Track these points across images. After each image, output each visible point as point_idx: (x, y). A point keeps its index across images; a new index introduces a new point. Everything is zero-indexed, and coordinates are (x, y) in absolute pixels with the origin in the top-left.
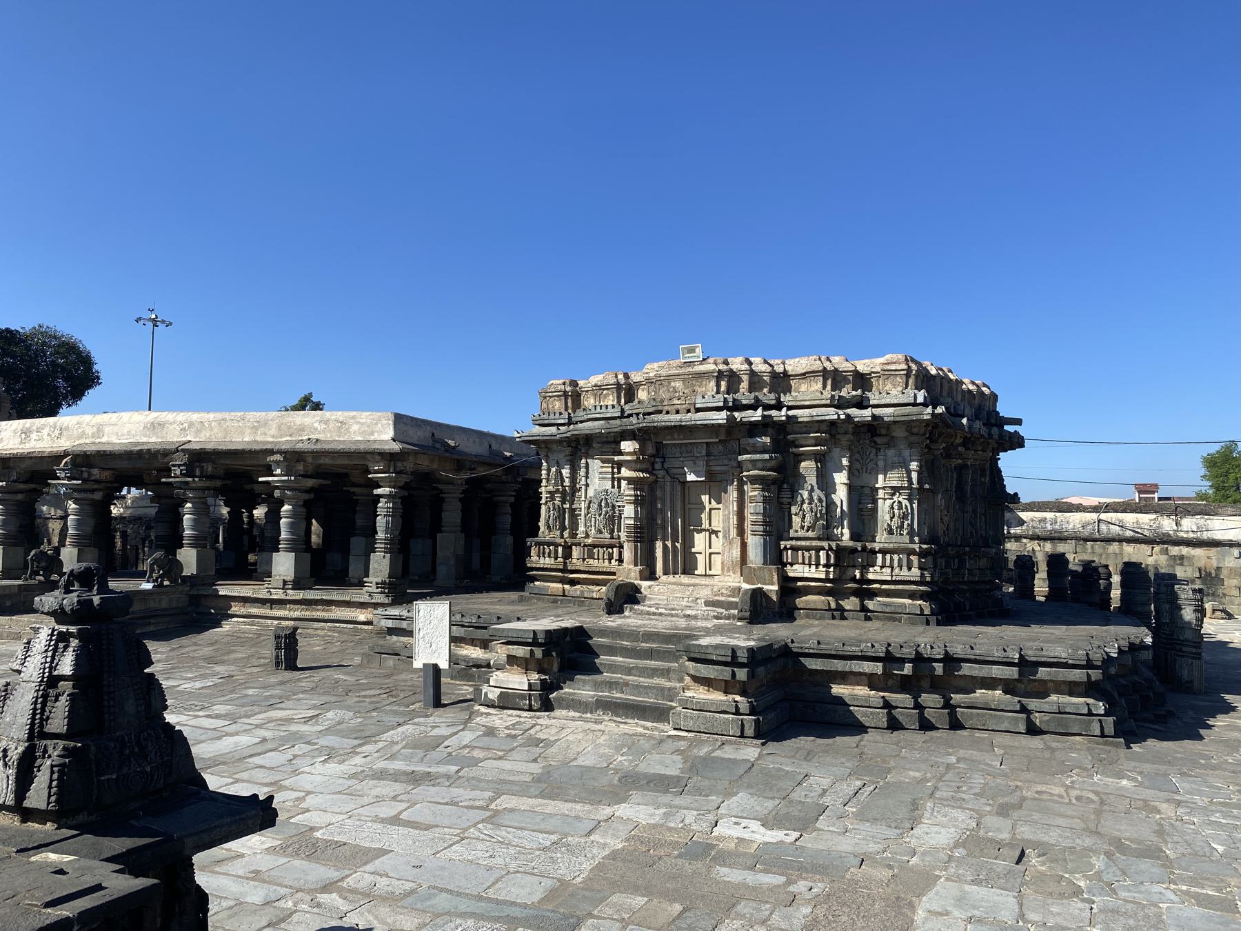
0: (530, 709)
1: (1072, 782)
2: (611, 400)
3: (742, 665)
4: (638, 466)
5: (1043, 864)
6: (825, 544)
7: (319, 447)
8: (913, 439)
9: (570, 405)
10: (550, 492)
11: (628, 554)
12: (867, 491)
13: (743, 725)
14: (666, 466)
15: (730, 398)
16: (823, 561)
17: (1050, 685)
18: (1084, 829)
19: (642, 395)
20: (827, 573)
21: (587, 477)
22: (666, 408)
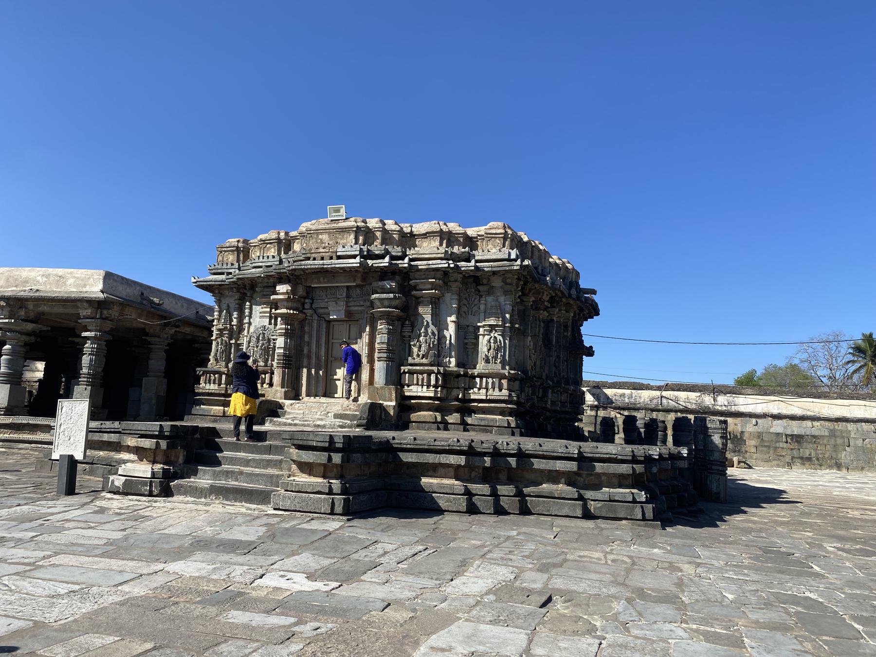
0: (151, 494)
1: (612, 550)
2: (273, 251)
3: (337, 450)
4: (290, 304)
5: (567, 608)
6: (435, 369)
7: (37, 294)
8: (508, 287)
9: (241, 259)
10: (219, 330)
11: (277, 379)
12: (471, 329)
13: (333, 504)
14: (314, 306)
15: (365, 248)
16: (433, 382)
17: (603, 478)
18: (612, 582)
19: (297, 247)
20: (436, 392)
21: (250, 317)
22: (313, 255)
